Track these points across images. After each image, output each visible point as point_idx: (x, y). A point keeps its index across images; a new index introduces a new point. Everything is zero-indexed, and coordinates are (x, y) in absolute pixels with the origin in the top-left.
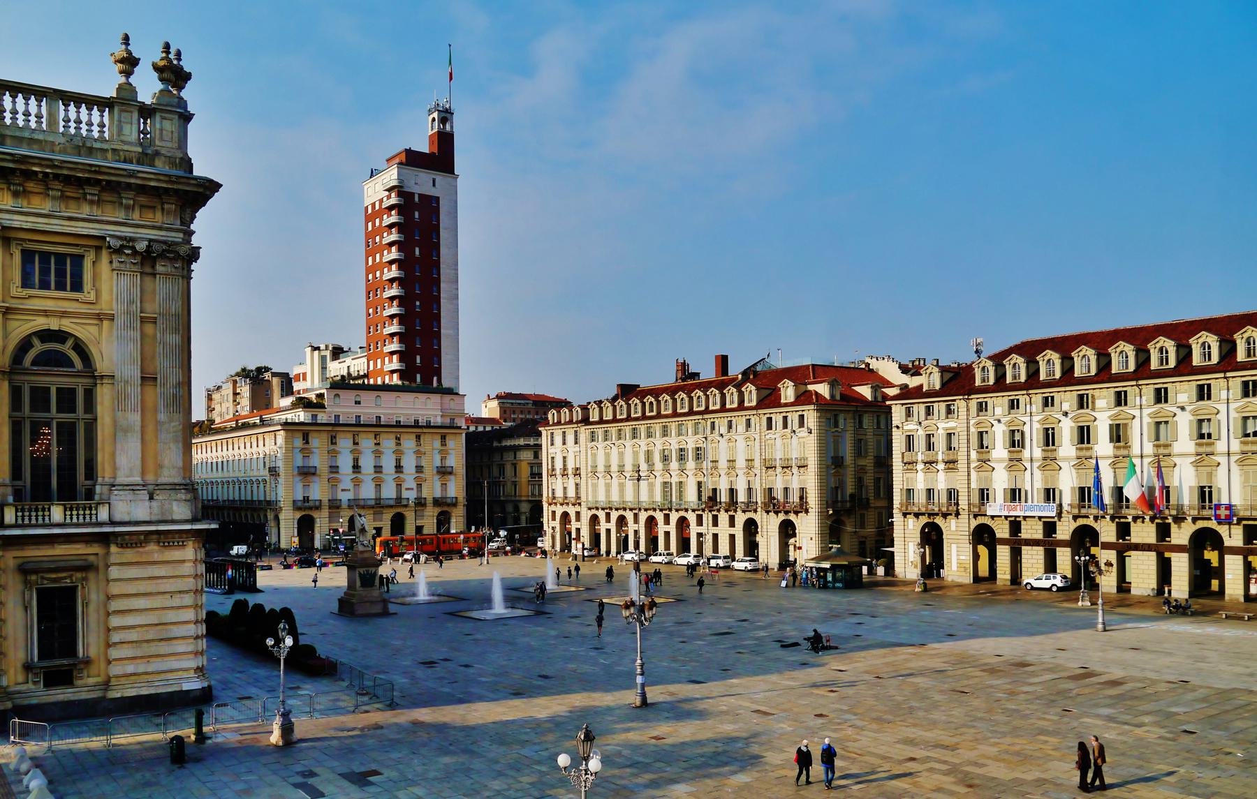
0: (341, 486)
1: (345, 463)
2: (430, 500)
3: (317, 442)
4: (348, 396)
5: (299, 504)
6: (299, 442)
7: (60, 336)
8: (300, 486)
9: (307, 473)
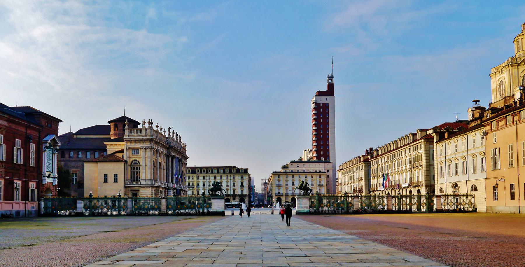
0: (289, 190)
1: (290, 183)
3: (282, 178)
6: (277, 178)
7: (136, 160)
9: (279, 186)
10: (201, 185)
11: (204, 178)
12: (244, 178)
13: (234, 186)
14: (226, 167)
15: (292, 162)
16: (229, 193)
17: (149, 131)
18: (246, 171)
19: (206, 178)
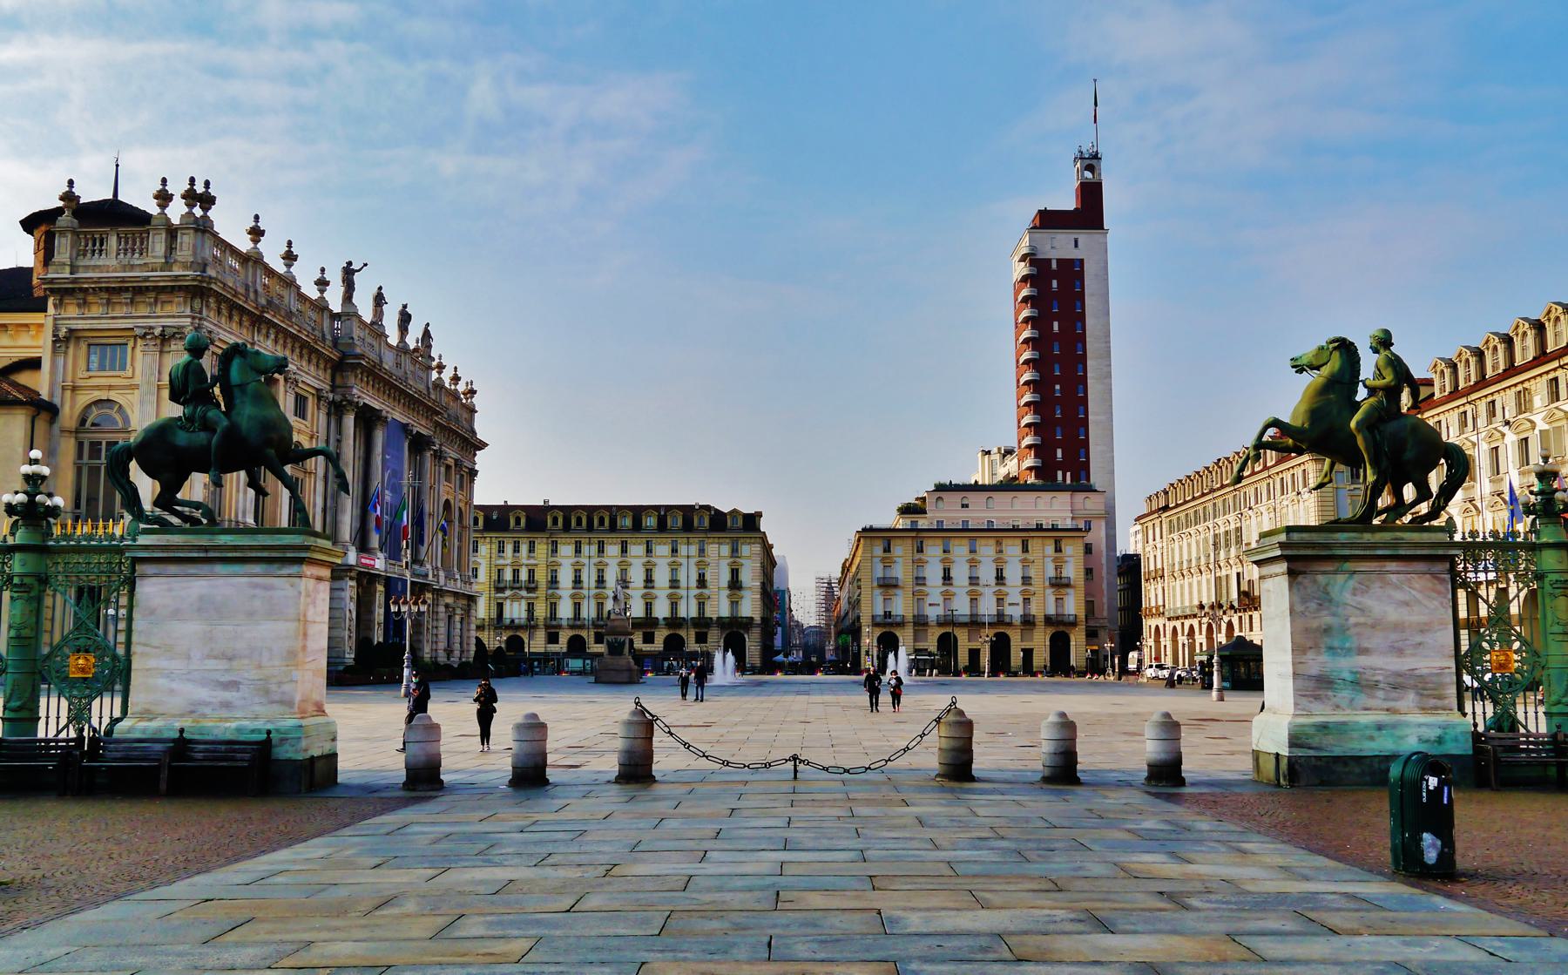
0: (929, 600)
1: (933, 573)
2: (1040, 619)
3: (901, 550)
4: (954, 499)
5: (878, 620)
6: (878, 550)
8: (880, 599)
9: (888, 585)
10: (566, 578)
11: (578, 551)
12: (745, 550)
13: (702, 582)
14: (669, 508)
15: (940, 488)
16: (682, 613)
17: (186, 240)
18: (751, 522)
19: (585, 549)
